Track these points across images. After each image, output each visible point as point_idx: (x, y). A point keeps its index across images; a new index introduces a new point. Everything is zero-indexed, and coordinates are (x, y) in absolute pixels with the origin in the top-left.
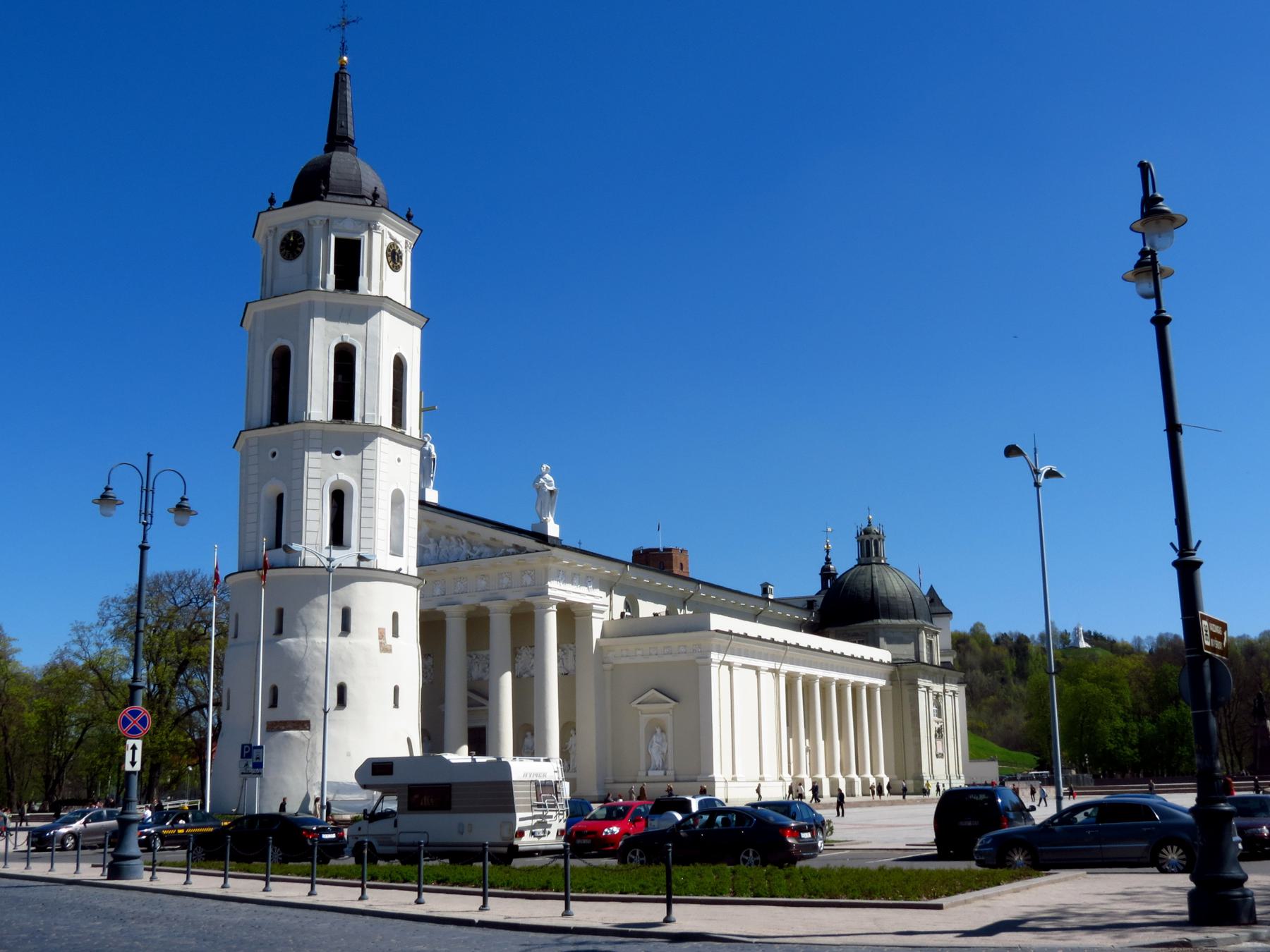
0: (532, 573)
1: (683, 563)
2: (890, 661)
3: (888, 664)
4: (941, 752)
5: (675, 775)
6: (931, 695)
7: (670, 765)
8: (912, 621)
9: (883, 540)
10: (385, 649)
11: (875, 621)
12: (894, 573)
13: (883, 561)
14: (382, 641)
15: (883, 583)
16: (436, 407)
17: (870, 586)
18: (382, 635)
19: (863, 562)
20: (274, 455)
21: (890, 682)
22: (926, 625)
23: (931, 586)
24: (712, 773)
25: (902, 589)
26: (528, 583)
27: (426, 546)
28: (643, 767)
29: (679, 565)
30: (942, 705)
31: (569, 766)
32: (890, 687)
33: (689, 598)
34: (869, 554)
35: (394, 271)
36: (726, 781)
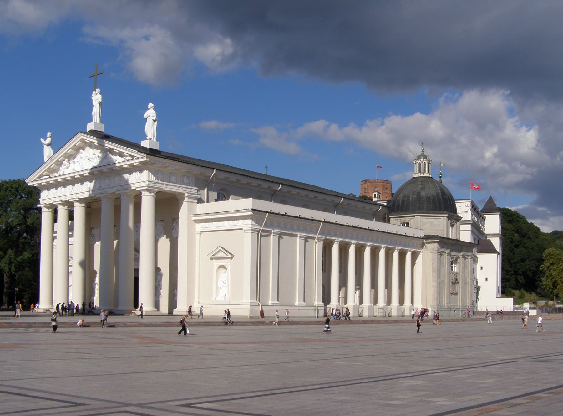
2: (423, 236)
25: (436, 193)
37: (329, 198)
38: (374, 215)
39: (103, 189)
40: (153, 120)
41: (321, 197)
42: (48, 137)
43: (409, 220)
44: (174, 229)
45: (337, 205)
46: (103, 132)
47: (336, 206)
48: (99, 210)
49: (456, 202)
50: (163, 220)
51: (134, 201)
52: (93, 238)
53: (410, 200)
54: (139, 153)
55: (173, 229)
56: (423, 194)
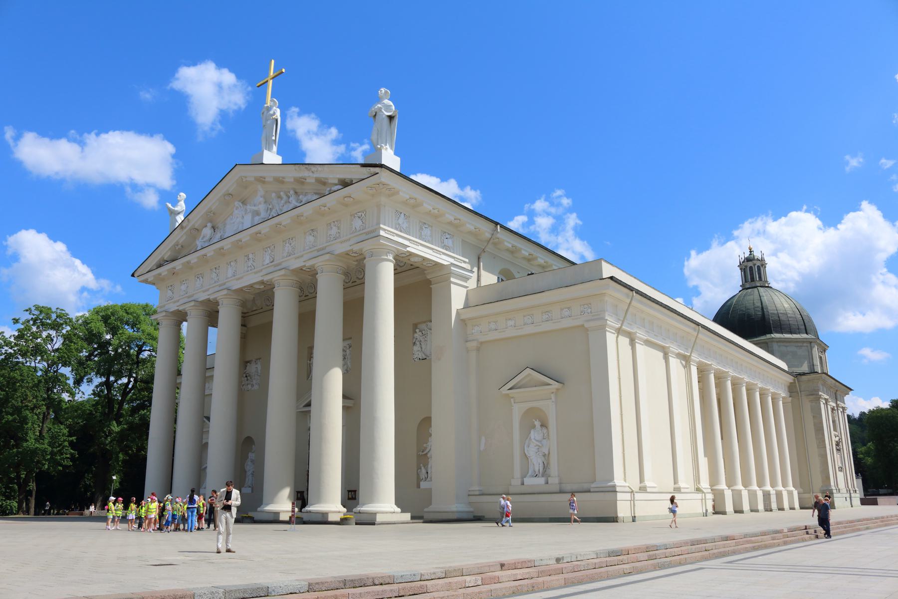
0: (363, 214)
5: (560, 483)
7: (554, 470)
8: (805, 336)
9: (765, 267)
11: (768, 336)
13: (767, 285)
16: (284, 70)
17: (759, 304)
19: (748, 286)
24: (612, 479)
26: (358, 228)
27: (255, 208)
28: (517, 474)
31: (427, 473)
34: (753, 280)
36: (632, 492)
44: (418, 343)
52: (247, 380)
55: (414, 343)
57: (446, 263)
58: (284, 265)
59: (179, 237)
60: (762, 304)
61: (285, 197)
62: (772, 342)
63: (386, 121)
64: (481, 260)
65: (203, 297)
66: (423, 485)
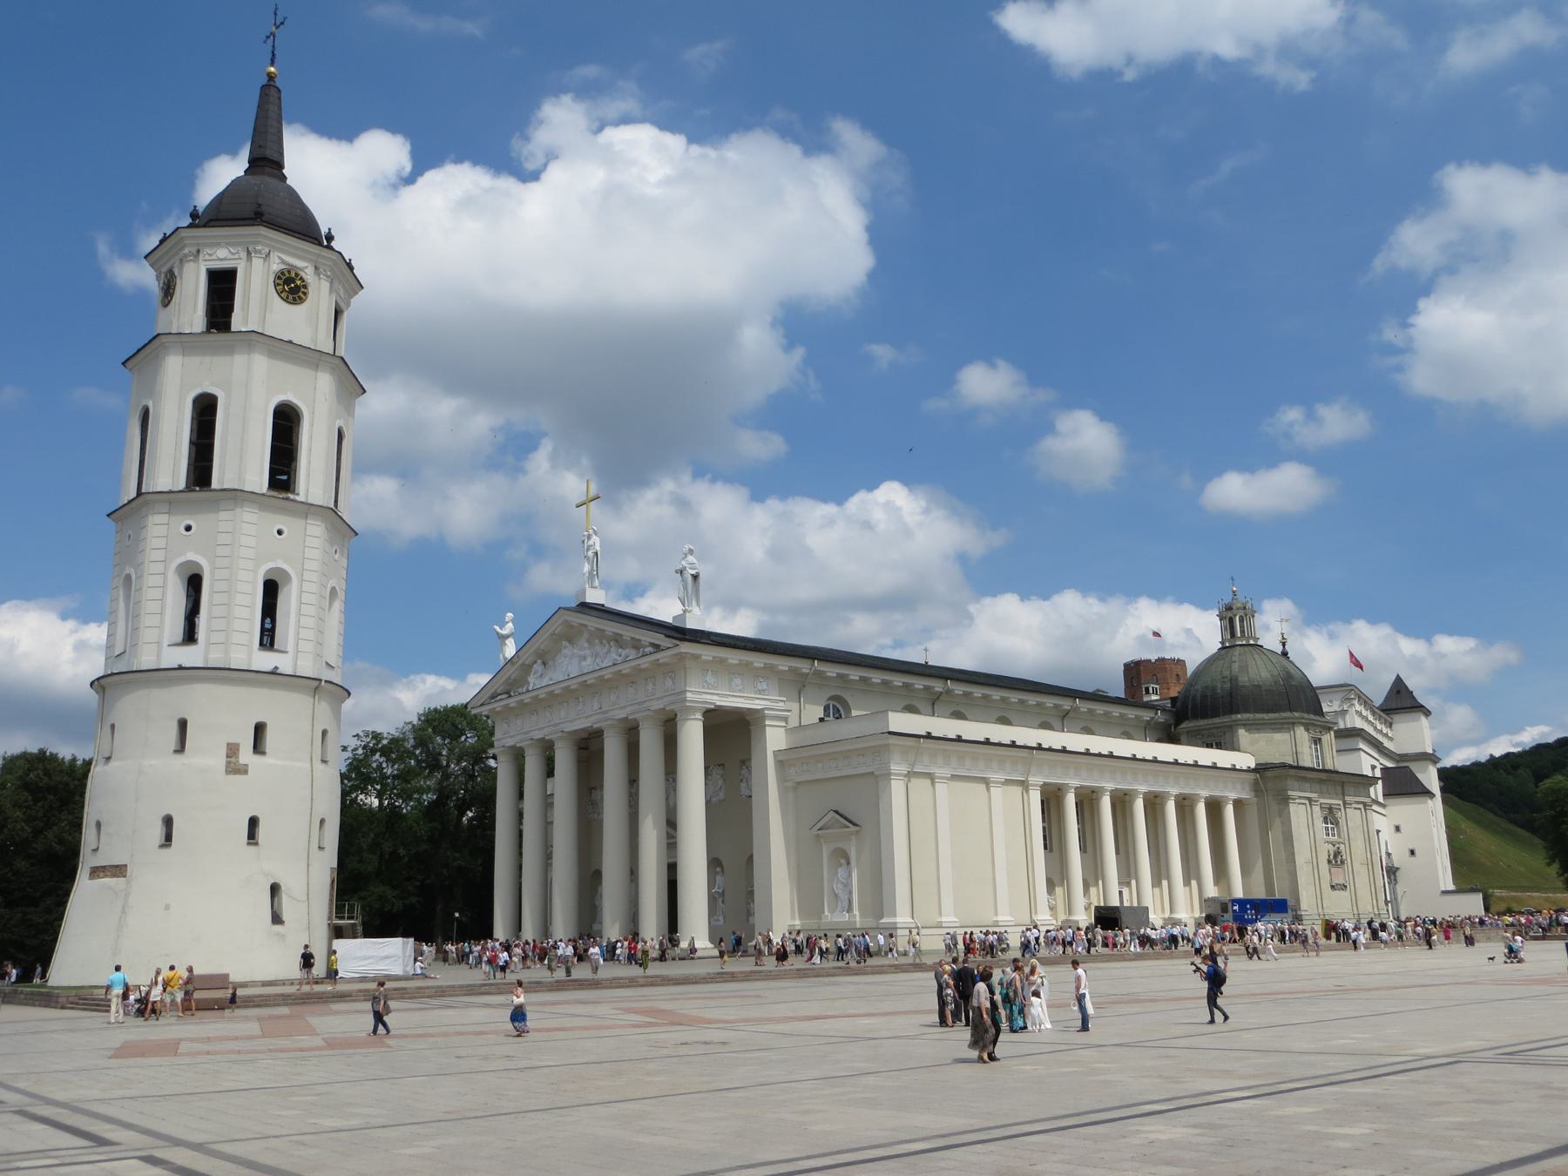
1: (1179, 673)
3: (1249, 770)
4: (1341, 881)
6: (1317, 809)
8: (1288, 714)
9: (1253, 616)
10: (235, 768)
11: (1234, 717)
12: (1263, 656)
13: (1252, 642)
14: (233, 759)
15: (1244, 669)
17: (1229, 673)
18: (233, 750)
20: (129, 536)
21: (1253, 793)
22: (1303, 718)
23: (1398, 675)
25: (1272, 675)
27: (582, 653)
29: (1174, 676)
30: (1342, 822)
32: (1255, 799)
33: (938, 698)
34: (1233, 634)
35: (290, 303)
36: (918, 928)
37: (1050, 701)
38: (1145, 730)
39: (606, 712)
40: (692, 575)
41: (1032, 699)
42: (508, 622)
43: (1221, 736)
45: (1067, 714)
46: (603, 605)
47: (1064, 717)
48: (600, 753)
49: (1317, 691)
50: (723, 765)
51: (665, 731)
53: (1217, 693)
54: (667, 639)
55: (742, 780)
56: (1243, 679)
57: (760, 707)
58: (611, 714)
59: (512, 672)
60: (1231, 672)
61: (607, 645)
62: (1238, 725)
63: (690, 579)
64: (802, 695)
65: (538, 735)
66: (750, 918)
